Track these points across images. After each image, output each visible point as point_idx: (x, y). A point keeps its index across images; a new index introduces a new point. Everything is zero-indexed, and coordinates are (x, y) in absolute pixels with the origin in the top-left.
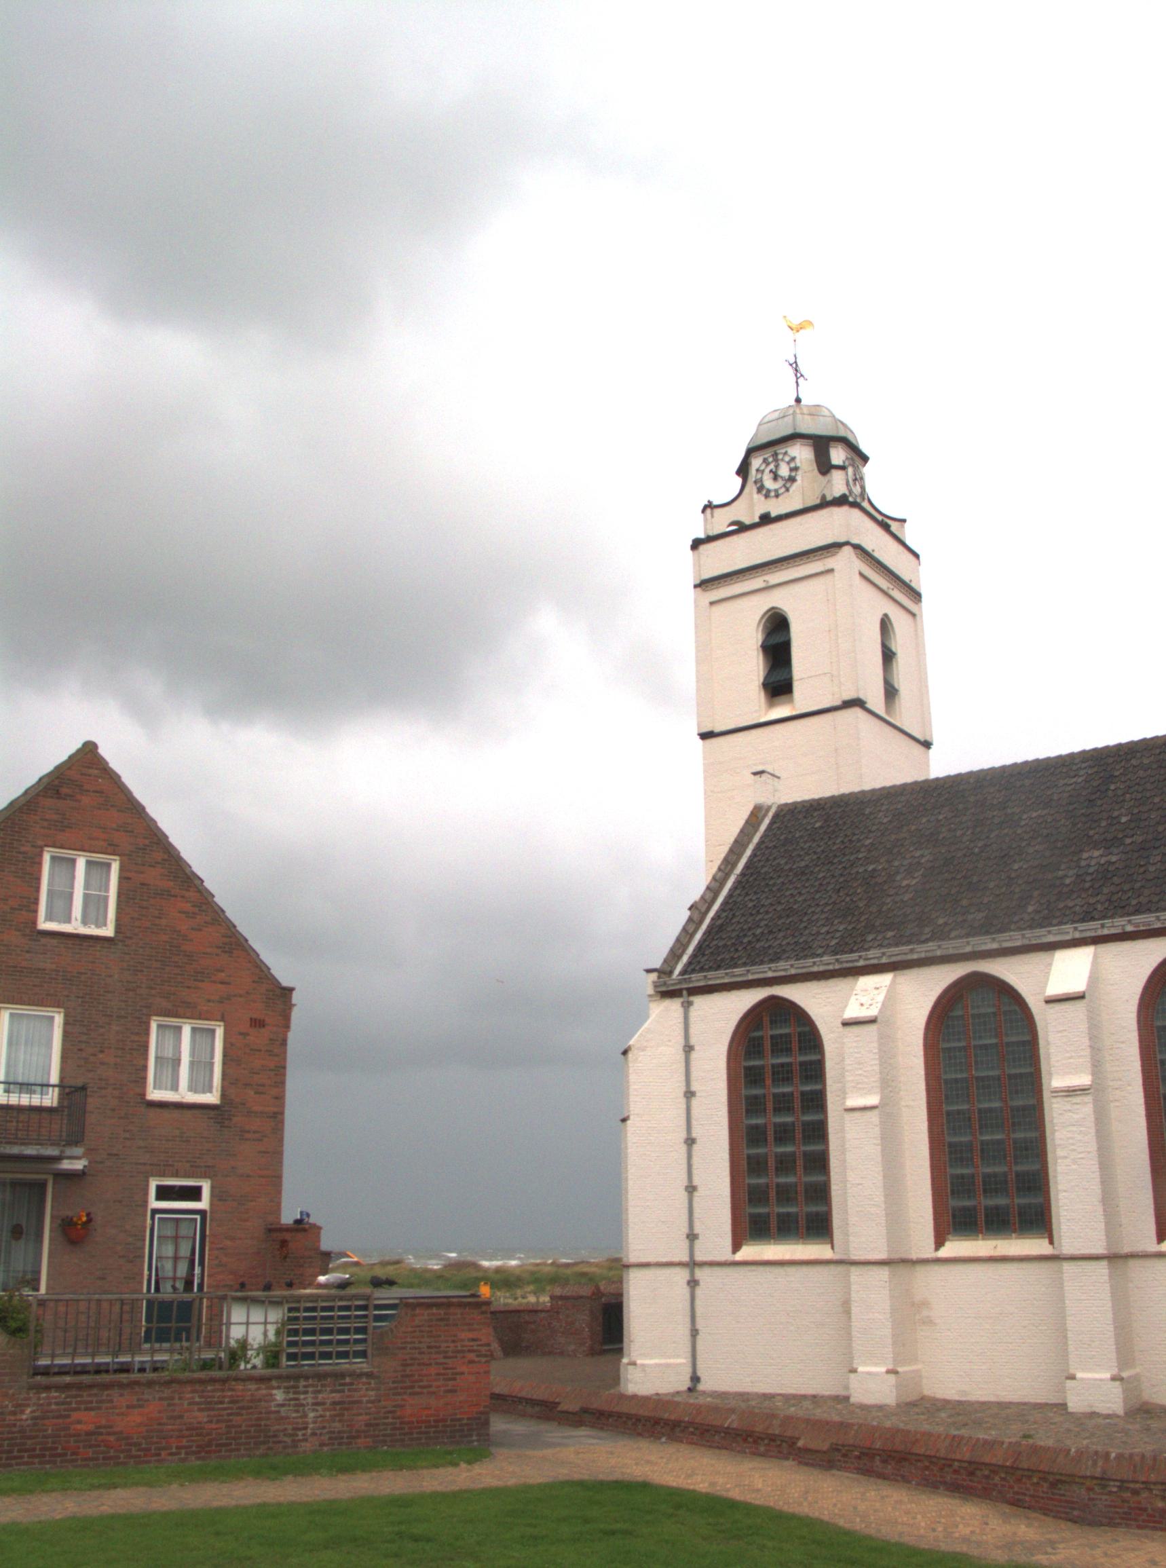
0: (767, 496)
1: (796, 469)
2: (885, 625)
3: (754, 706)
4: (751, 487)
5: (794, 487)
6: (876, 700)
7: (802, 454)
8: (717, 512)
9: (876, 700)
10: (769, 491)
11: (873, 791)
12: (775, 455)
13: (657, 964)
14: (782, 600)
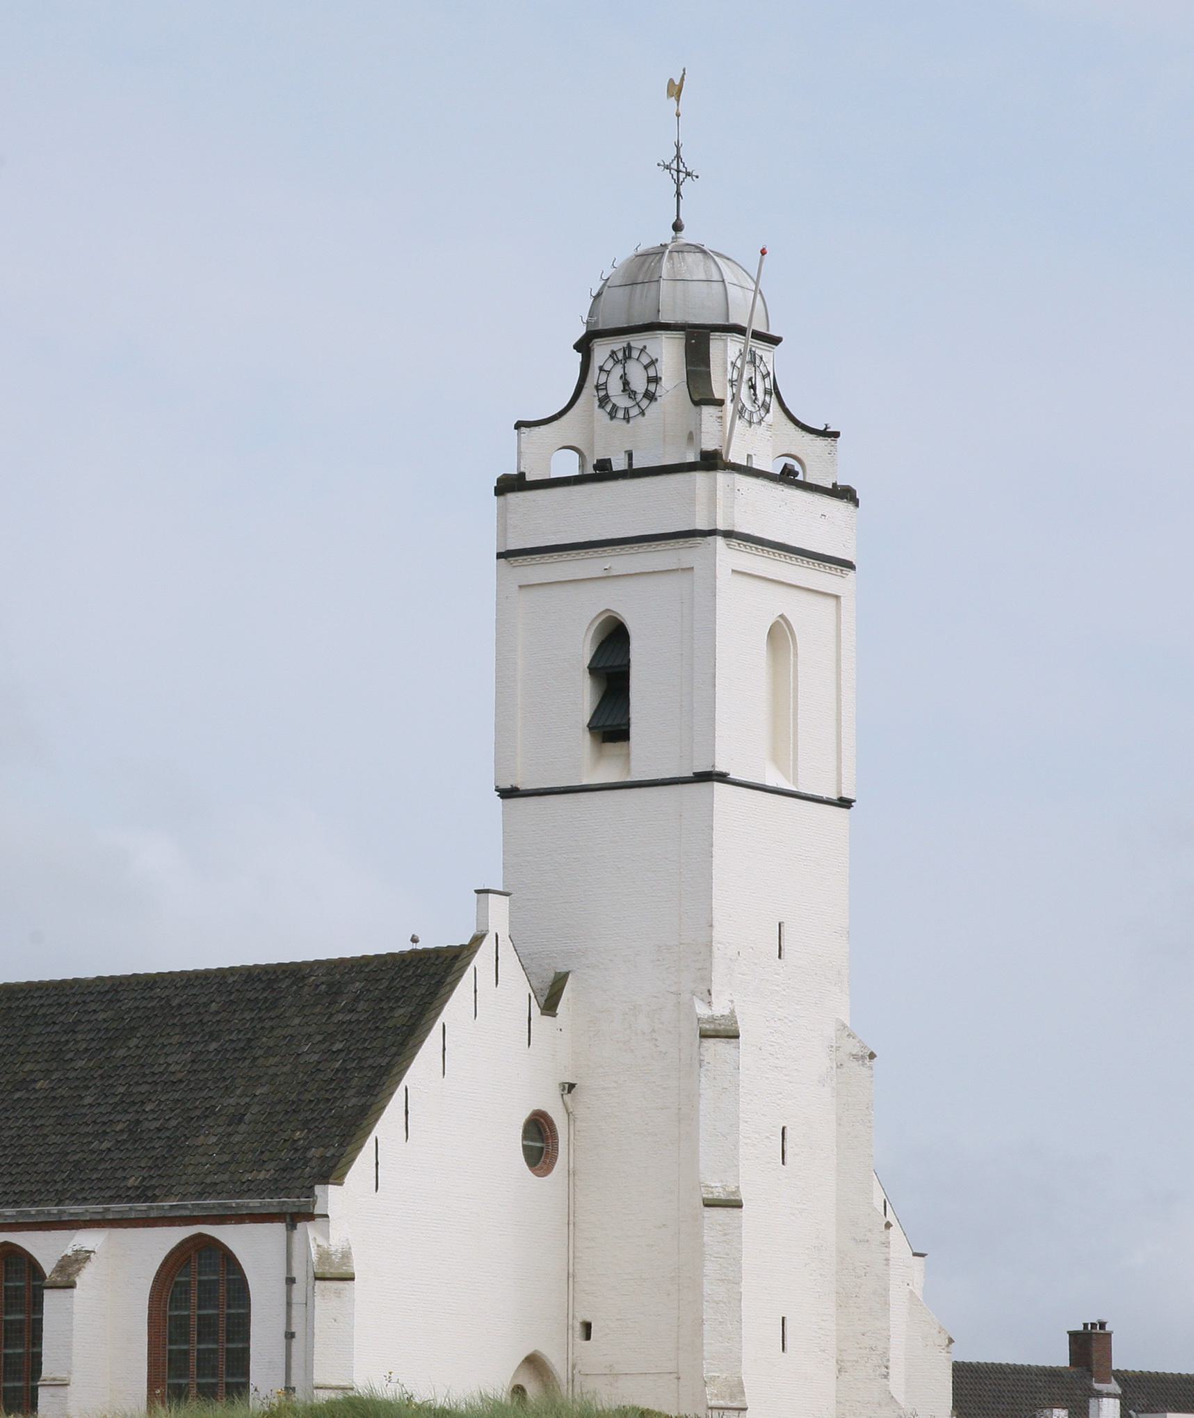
0: (612, 415)
2: (779, 635)
3: (581, 760)
5: (653, 410)
7: (668, 353)
10: (615, 408)
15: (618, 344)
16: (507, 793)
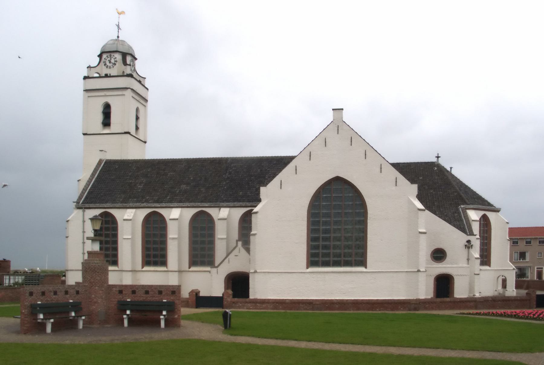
0: (107, 67)
1: (116, 61)
4: (102, 63)
5: (115, 67)
6: (133, 132)
7: (118, 57)
8: (92, 69)
9: (133, 132)
11: (132, 160)
12: (111, 55)
13: (75, 201)
14: (110, 100)
15: (108, 54)
16: (84, 134)
